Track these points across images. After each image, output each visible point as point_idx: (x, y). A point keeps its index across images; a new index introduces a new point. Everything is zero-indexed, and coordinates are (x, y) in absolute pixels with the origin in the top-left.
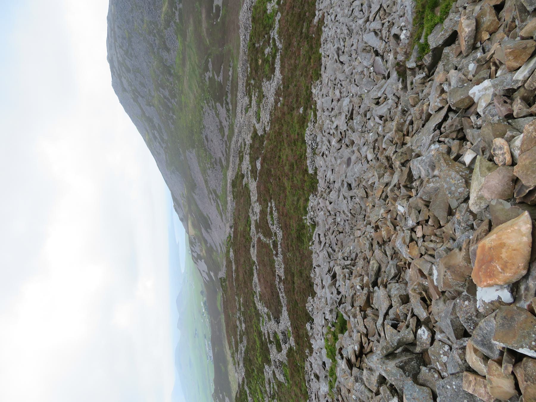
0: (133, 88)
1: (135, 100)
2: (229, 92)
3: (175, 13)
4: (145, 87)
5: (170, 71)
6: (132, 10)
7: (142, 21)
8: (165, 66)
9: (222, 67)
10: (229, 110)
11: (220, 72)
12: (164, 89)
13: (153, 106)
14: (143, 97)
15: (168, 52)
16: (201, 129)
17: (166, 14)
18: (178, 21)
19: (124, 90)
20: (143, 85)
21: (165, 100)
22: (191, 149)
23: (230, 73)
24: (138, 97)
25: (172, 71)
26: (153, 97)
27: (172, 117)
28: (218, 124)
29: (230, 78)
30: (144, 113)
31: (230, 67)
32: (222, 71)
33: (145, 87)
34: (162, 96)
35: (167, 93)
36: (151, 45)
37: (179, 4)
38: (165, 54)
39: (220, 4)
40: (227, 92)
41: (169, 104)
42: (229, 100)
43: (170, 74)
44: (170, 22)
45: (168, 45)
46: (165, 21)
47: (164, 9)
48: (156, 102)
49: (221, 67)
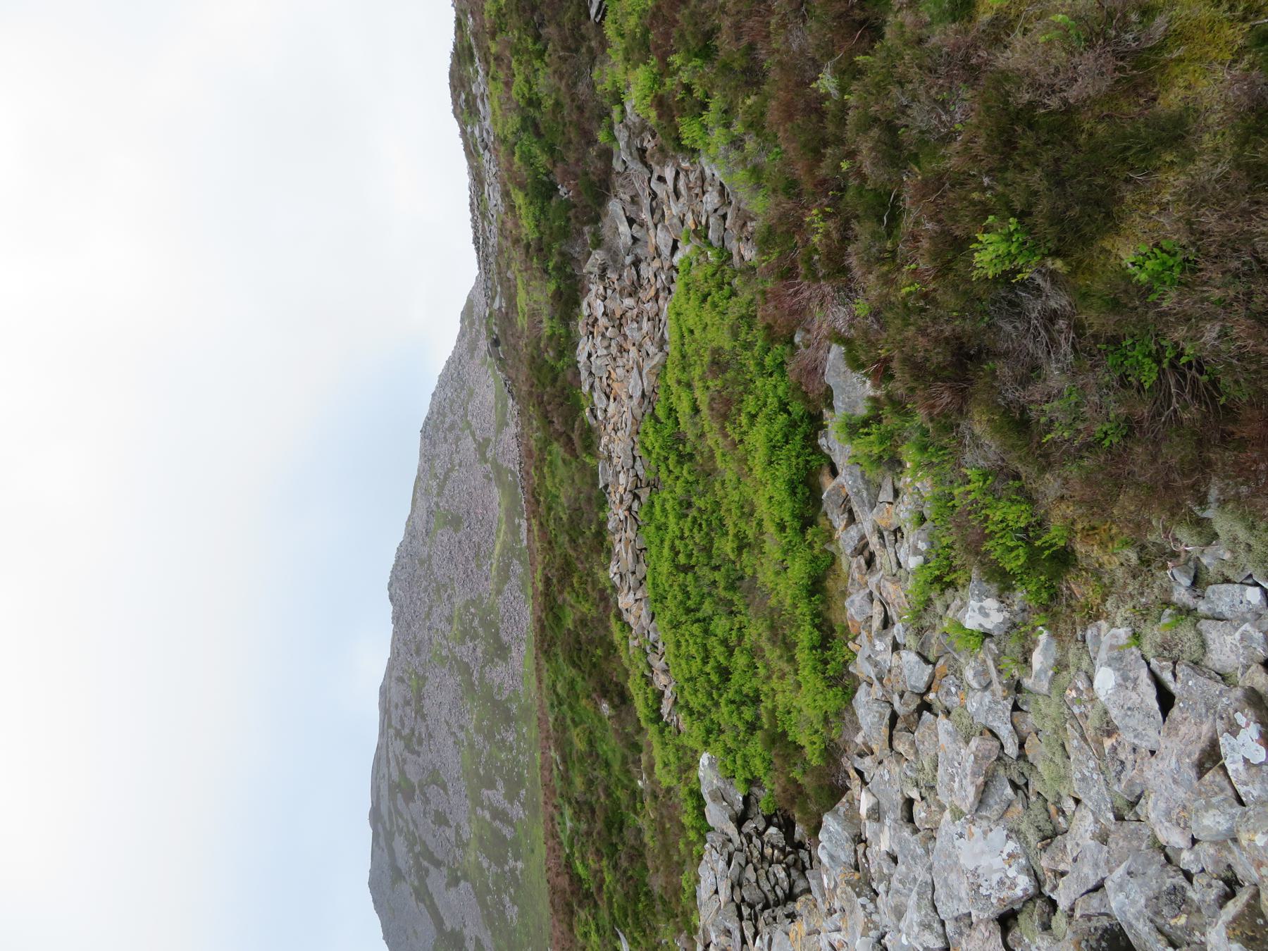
0: (418, 848)
1: (422, 894)
3: (520, 525)
4: (447, 823)
5: (509, 710)
6: (431, 608)
7: (450, 620)
8: (496, 704)
12: (491, 785)
13: (465, 877)
14: (438, 864)
15: (505, 659)
17: (502, 555)
19: (398, 875)
20: (441, 819)
21: (497, 823)
24: (427, 871)
25: (514, 708)
26: (463, 845)
27: (513, 871)
30: (439, 921)
33: (447, 823)
34: (488, 816)
35: (497, 796)
36: (466, 669)
38: (499, 674)
41: (507, 832)
43: (508, 718)
44: (509, 566)
45: (505, 638)
46: (499, 573)
47: (498, 547)
48: (474, 856)
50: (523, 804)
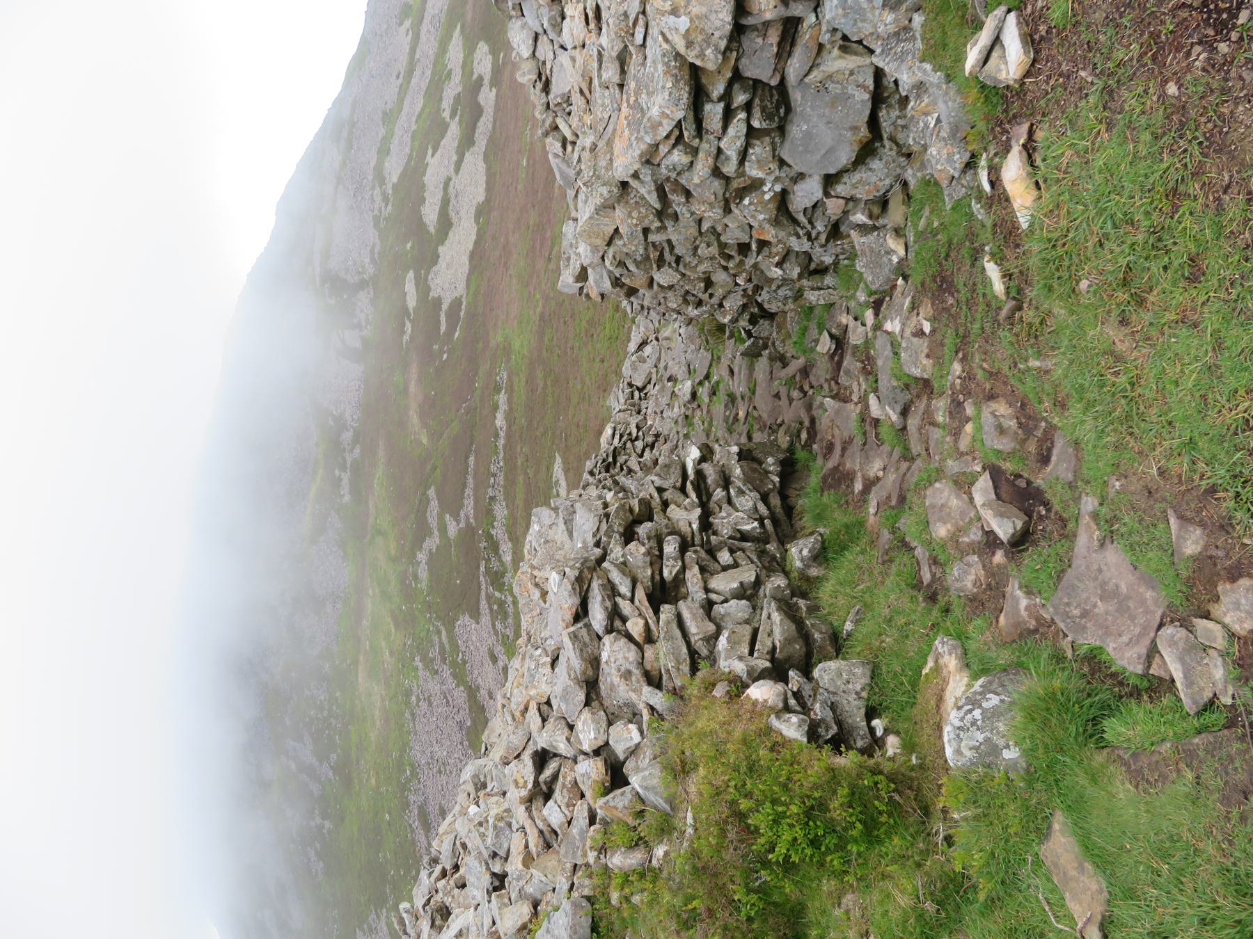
2: (501, 497)
3: (340, 479)
9: (472, 460)
10: (503, 576)
11: (465, 485)
16: (404, 788)
18: (347, 498)
22: (373, 916)
23: (500, 421)
28: (464, 714)
29: (502, 442)
31: (497, 389)
32: (470, 481)
34: (293, 767)
37: (351, 451)
39: (461, 289)
40: (492, 498)
42: (499, 532)
49: (467, 466)
50: (332, 768)
